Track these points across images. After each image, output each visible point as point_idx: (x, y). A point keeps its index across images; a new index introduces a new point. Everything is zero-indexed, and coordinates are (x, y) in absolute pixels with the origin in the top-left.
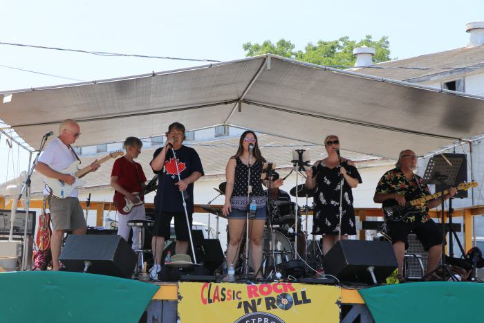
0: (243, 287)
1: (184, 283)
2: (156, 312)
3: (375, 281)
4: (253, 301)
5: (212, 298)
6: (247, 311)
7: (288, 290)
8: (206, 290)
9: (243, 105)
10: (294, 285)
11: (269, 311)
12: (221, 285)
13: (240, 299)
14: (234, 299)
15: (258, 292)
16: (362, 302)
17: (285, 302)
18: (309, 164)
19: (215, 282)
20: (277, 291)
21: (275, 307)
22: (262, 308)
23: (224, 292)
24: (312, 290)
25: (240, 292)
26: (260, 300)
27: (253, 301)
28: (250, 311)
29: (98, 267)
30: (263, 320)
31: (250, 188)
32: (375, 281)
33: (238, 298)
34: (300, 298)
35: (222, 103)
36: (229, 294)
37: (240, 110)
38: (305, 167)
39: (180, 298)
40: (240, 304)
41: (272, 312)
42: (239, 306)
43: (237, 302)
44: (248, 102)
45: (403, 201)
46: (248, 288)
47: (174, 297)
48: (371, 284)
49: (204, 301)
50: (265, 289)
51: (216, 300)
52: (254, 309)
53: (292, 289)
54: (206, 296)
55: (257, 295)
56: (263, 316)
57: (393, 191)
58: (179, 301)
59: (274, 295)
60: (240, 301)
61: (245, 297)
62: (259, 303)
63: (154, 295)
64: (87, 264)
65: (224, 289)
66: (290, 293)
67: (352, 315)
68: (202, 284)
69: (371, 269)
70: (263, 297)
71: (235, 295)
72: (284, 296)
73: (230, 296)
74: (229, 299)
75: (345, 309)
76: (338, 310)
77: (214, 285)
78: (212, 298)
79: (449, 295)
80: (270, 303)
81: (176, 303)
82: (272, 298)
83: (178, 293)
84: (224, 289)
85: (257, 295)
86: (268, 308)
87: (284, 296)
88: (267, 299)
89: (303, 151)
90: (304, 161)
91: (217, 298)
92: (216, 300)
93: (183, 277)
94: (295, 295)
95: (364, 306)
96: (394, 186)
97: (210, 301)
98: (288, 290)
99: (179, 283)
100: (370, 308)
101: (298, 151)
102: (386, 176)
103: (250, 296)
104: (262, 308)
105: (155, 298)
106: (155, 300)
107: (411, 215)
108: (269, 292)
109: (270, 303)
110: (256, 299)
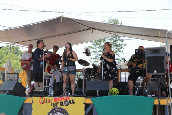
0: (53, 98)
1: (34, 97)
2: (26, 107)
3: (98, 95)
4: (56, 103)
5: (43, 102)
6: (54, 107)
7: (68, 99)
8: (41, 99)
9: (94, 30)
10: (70, 97)
11: (61, 106)
12: (46, 98)
13: (52, 102)
14: (50, 102)
15: (58, 100)
16: (92, 103)
17: (67, 103)
18: (90, 53)
19: (44, 96)
20: (64, 99)
21: (63, 105)
22: (59, 105)
23: (47, 100)
24: (76, 99)
25: (52, 100)
26: (58, 103)
27: (56, 103)
28: (55, 106)
29: (11, 93)
30: (59, 109)
31: (66, 63)
32: (98, 95)
33: (51, 102)
34: (72, 102)
35: (85, 30)
36: (48, 101)
37: (92, 32)
38: (89, 54)
39: (33, 102)
40: (52, 104)
41: (62, 107)
42: (52, 105)
43: (51, 103)
44: (96, 29)
45: (134, 65)
46: (54, 98)
47: (31, 102)
48: (96, 96)
49: (40, 103)
50: (60, 99)
51: (44, 103)
52: (56, 106)
53: (69, 99)
54: (41, 102)
55: (57, 101)
56: (59, 108)
57: (133, 61)
58: (32, 103)
59: (63, 101)
60: (52, 103)
61: (53, 102)
62: (58, 104)
63: (24, 101)
64: (7, 91)
65: (47, 99)
66: (68, 100)
67: (89, 109)
68: (40, 97)
69: (98, 91)
70: (59, 102)
71: (50, 101)
72: (66, 101)
73: (48, 101)
74: (48, 102)
75: (87, 106)
76: (84, 106)
77: (43, 98)
78: (43, 102)
79: (122, 100)
80: (62, 104)
81: (32, 104)
82: (62, 102)
83: (32, 101)
84: (47, 99)
85: (57, 101)
86: (61, 105)
87: (66, 101)
88: (61, 102)
89: (87, 49)
90: (88, 52)
91: (45, 102)
92: (44, 103)
93: (34, 95)
94: (70, 101)
95: (93, 104)
96: (134, 60)
97: (42, 103)
98: (68, 99)
99: (33, 97)
100: (94, 105)
101: (86, 49)
102: (133, 56)
103: (55, 101)
104: (59, 105)
105: (24, 102)
106: (26, 103)
107: (137, 71)
108: (61, 100)
109: (62, 104)
110: (57, 102)
